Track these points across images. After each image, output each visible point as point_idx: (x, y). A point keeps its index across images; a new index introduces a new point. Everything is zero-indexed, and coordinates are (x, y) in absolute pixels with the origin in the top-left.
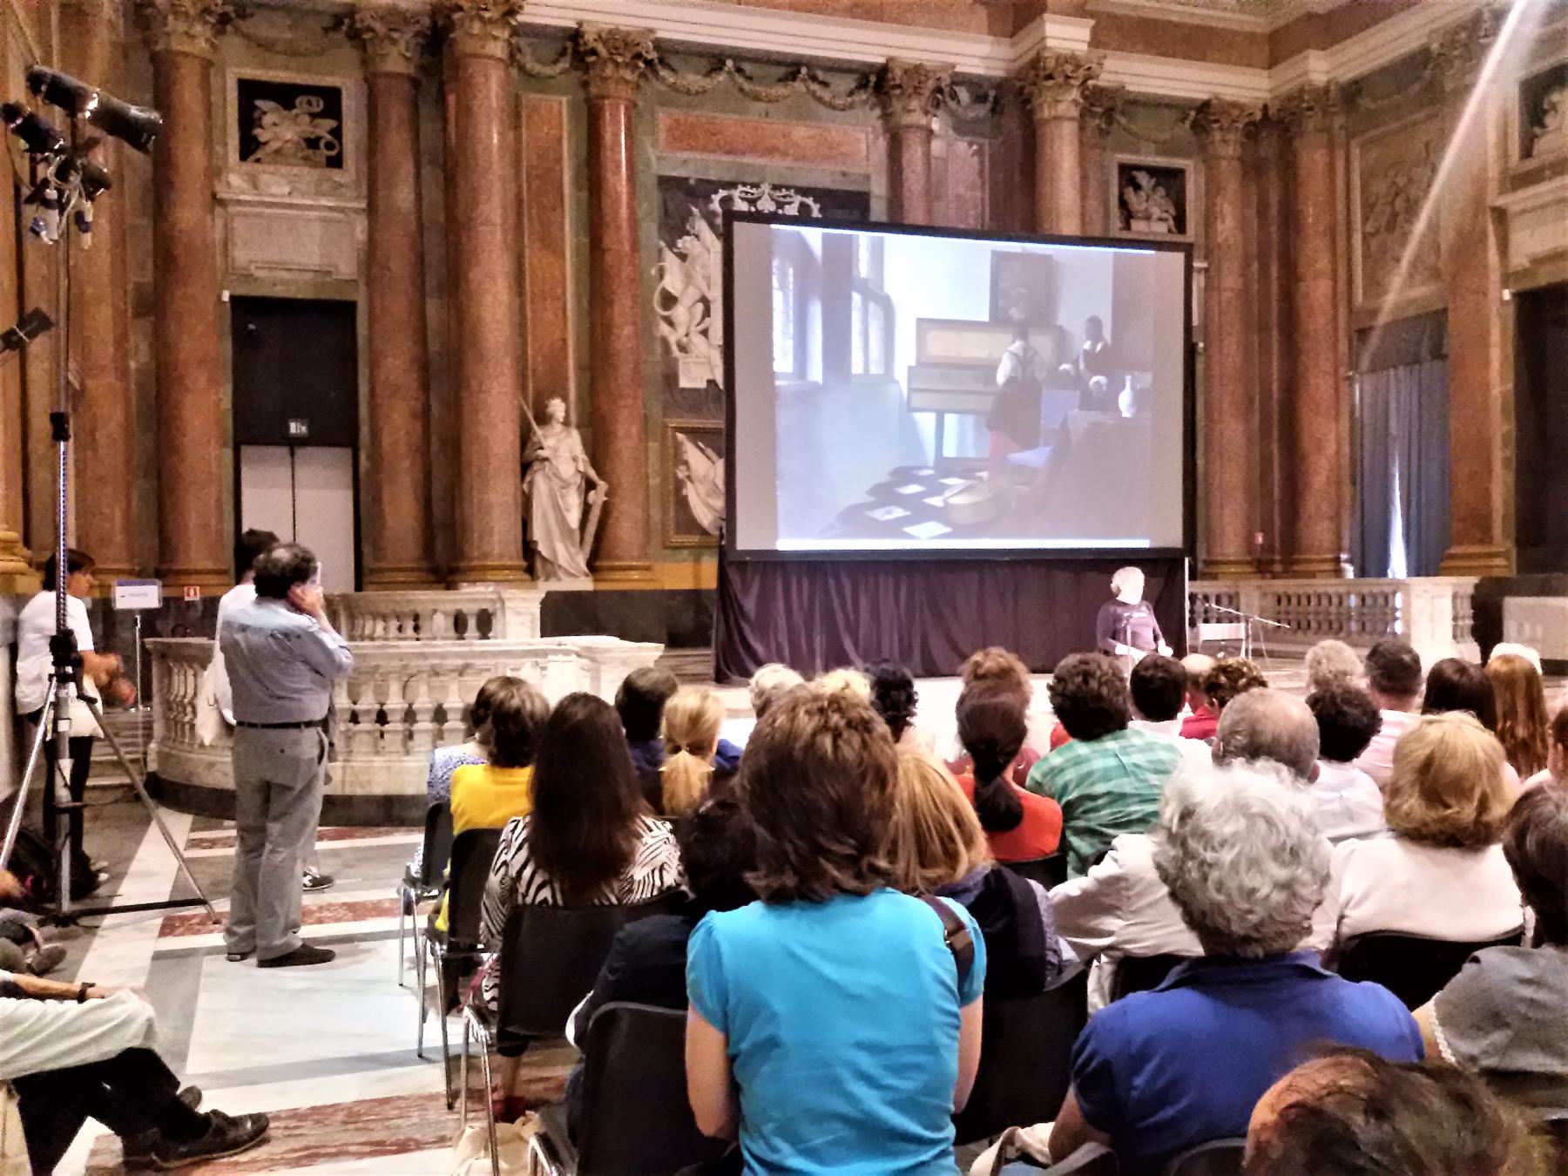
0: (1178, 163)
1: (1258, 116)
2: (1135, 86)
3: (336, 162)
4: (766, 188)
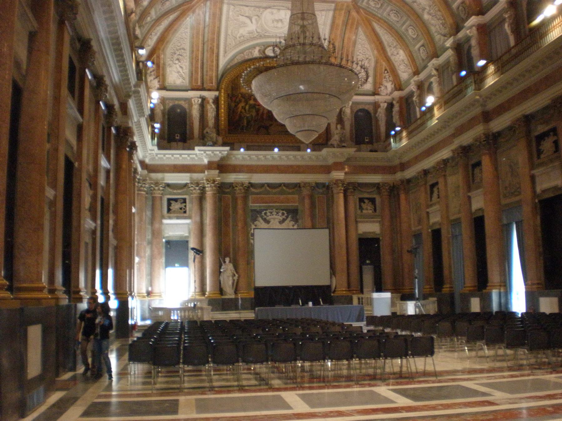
0: (374, 196)
1: (392, 185)
2: (361, 181)
3: (185, 212)
4: (274, 210)
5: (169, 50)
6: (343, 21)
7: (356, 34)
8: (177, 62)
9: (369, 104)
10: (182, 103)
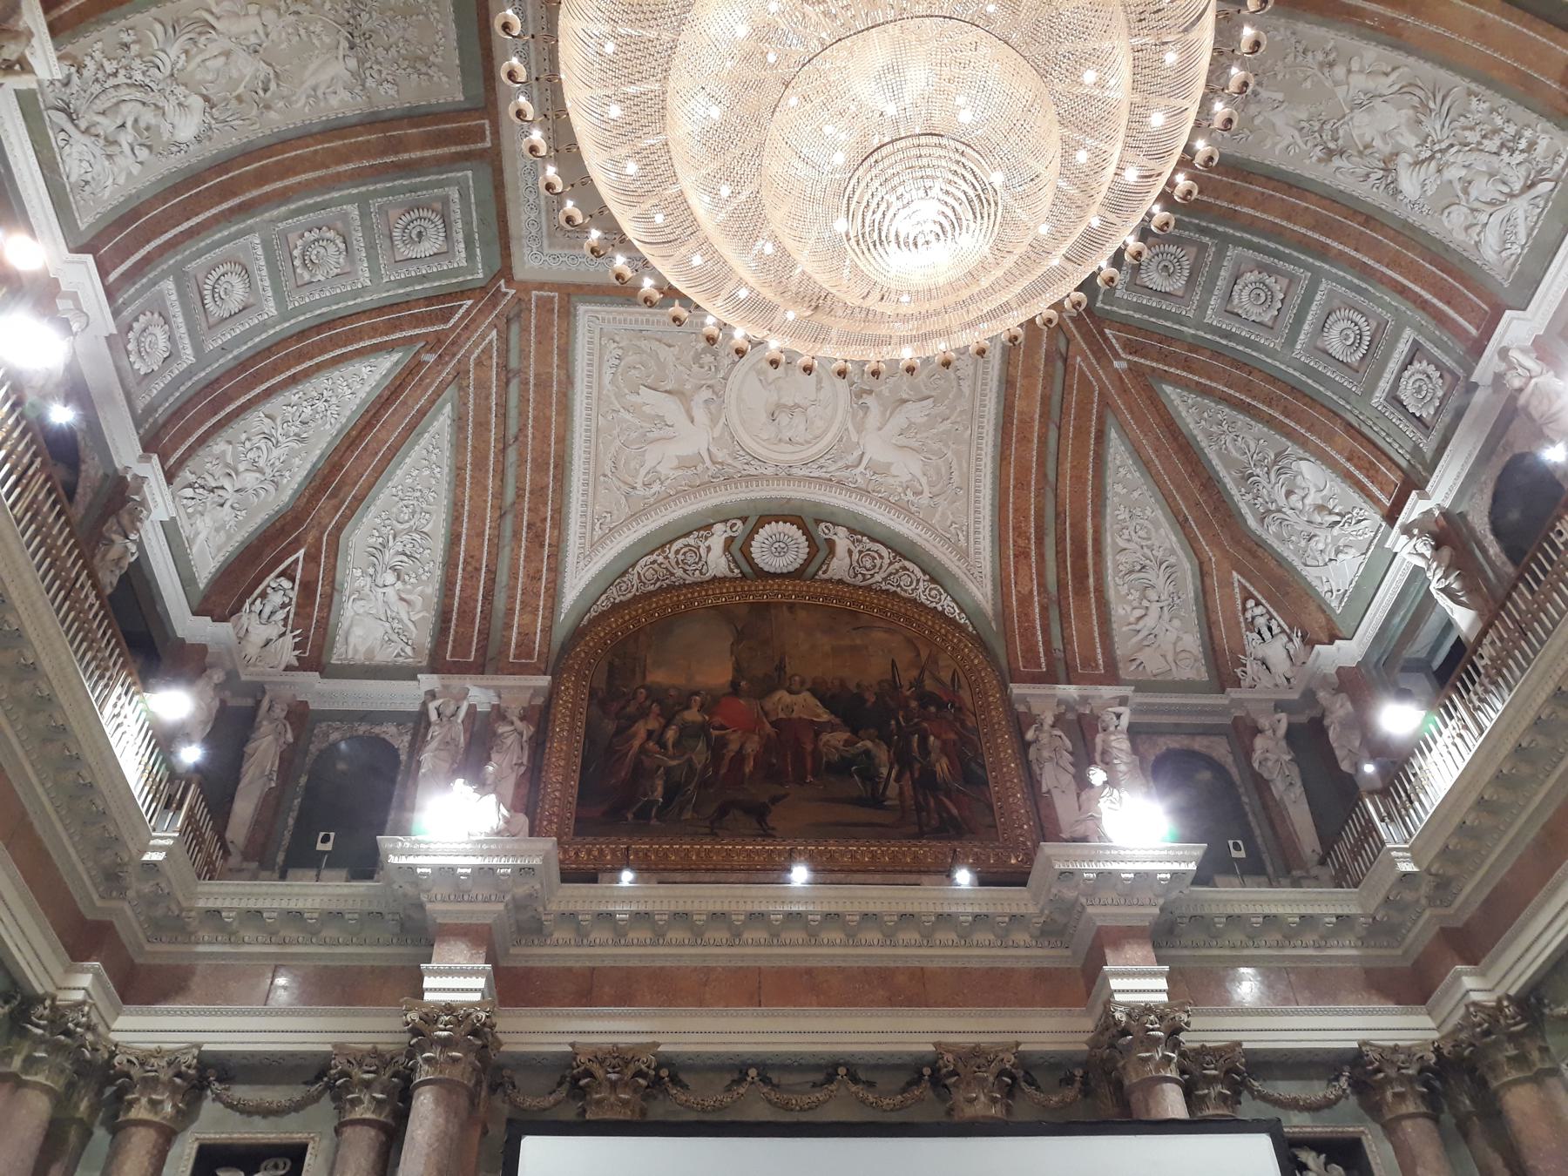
5: (360, 537)
6: (1046, 400)
7: (1100, 460)
8: (390, 578)
9: (1207, 731)
10: (389, 731)
